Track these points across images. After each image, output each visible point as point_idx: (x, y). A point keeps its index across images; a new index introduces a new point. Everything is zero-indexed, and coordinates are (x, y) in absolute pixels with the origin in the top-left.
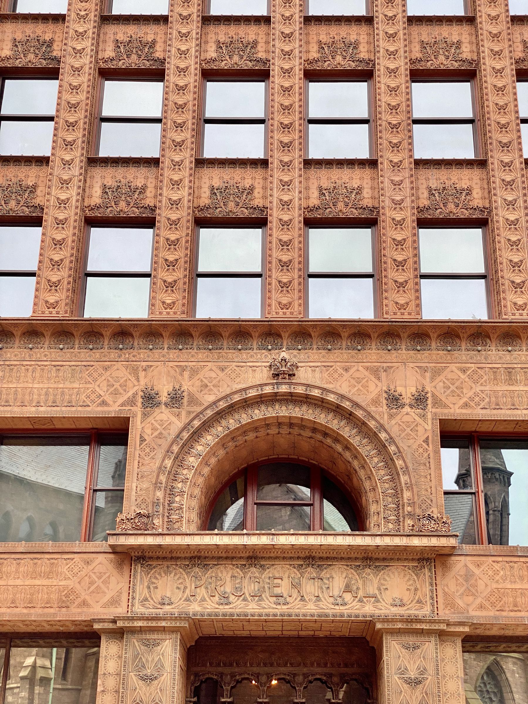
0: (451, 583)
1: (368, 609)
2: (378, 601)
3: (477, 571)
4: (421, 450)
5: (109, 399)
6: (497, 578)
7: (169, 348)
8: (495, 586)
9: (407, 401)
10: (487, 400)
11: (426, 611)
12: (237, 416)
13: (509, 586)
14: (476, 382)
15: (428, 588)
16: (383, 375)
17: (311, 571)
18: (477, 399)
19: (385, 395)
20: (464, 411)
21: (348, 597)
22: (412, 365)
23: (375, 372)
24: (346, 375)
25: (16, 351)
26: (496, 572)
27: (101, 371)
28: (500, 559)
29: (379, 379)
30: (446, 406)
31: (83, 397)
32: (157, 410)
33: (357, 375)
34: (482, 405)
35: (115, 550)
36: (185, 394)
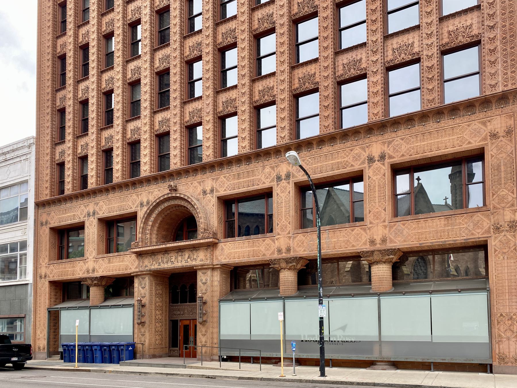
0: (218, 252)
1: (194, 263)
9: (208, 192)
11: (208, 262)
13: (233, 251)
14: (228, 181)
16: (202, 183)
17: (180, 253)
20: (224, 192)
21: (189, 260)
23: (199, 183)
24: (192, 186)
26: (230, 247)
30: (219, 192)
33: (195, 185)
34: (230, 189)
35: (136, 253)
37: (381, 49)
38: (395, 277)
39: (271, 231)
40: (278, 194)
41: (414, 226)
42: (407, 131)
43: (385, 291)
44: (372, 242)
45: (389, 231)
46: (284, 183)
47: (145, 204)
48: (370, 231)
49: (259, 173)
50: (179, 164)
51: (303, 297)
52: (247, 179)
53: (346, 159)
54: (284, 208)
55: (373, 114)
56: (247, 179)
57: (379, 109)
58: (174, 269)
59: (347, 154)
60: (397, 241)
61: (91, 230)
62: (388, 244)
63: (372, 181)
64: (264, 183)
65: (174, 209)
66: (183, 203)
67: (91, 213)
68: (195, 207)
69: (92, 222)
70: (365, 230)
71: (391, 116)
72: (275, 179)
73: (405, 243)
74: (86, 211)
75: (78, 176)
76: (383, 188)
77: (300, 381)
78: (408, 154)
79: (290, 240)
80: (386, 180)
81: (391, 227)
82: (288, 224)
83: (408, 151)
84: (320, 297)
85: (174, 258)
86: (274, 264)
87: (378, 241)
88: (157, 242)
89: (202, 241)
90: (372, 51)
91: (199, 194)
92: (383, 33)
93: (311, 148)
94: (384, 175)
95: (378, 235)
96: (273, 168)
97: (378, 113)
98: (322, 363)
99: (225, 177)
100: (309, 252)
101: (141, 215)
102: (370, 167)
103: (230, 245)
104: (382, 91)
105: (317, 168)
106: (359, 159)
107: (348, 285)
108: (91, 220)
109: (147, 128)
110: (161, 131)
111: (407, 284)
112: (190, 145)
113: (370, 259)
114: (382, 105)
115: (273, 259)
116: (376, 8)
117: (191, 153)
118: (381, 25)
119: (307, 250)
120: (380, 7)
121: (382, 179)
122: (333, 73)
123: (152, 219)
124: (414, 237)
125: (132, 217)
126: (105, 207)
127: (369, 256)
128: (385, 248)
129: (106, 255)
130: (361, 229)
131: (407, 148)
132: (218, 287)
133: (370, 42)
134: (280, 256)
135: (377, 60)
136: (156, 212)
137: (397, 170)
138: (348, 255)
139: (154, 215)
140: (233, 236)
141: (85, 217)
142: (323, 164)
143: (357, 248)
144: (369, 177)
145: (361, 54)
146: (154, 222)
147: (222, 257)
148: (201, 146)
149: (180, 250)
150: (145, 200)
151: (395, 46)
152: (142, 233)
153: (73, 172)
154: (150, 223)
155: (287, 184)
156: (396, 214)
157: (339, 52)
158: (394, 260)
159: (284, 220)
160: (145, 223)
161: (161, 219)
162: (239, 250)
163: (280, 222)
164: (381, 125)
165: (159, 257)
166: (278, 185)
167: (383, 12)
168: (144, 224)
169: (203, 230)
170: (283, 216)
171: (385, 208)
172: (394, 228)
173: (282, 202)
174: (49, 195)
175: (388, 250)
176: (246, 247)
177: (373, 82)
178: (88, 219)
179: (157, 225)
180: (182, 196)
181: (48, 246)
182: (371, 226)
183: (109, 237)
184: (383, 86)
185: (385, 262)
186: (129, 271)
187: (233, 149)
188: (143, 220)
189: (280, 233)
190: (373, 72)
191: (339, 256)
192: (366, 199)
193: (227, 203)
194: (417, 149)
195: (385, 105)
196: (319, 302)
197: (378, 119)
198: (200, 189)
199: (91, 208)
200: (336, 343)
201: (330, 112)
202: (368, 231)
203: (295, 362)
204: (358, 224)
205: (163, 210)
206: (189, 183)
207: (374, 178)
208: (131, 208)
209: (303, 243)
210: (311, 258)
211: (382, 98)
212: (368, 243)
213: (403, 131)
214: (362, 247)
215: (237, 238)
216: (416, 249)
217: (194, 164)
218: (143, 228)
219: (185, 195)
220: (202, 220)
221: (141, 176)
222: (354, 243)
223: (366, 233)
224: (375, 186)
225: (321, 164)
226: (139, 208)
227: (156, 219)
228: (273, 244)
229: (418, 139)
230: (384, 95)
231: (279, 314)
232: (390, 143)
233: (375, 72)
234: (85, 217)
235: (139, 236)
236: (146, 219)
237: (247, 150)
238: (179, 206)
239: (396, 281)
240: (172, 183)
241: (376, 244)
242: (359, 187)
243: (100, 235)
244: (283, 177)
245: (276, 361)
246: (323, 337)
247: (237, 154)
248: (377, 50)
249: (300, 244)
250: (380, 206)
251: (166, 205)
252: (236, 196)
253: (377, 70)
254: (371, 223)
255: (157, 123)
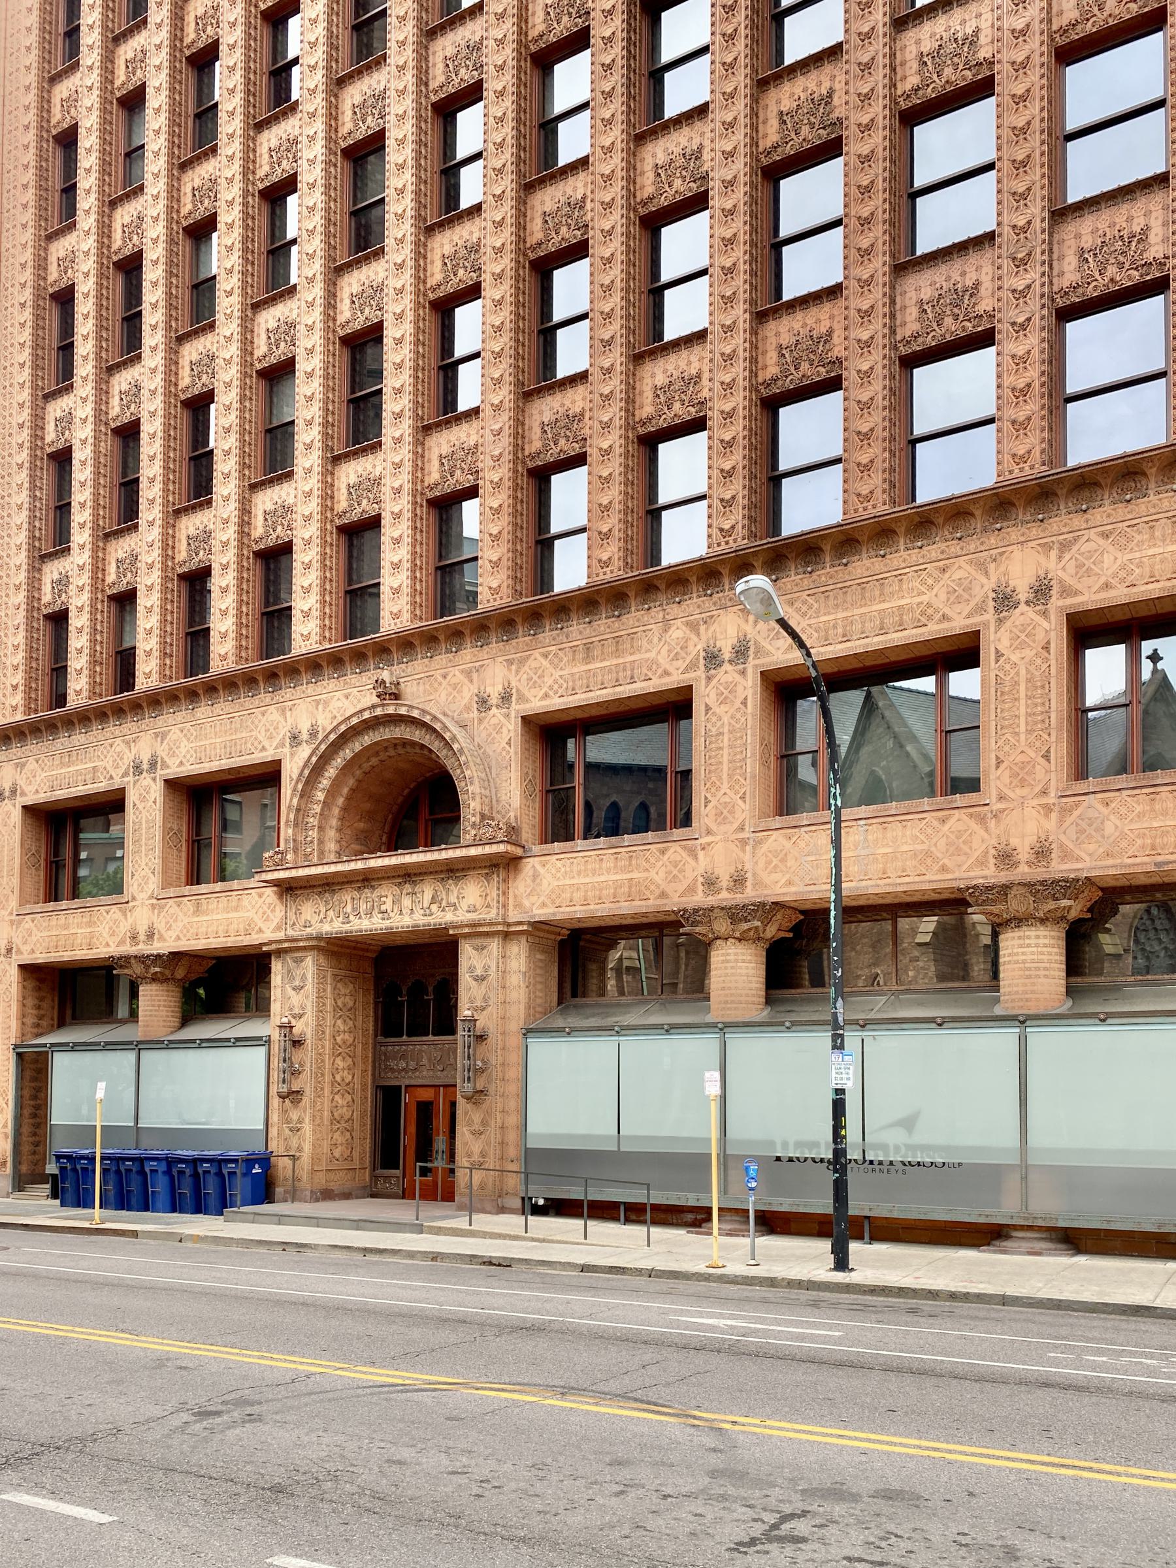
0: (521, 885)
2: (456, 909)
3: (541, 870)
4: (504, 753)
5: (266, 744)
6: (559, 875)
7: (307, 683)
8: (556, 883)
10: (565, 685)
11: (492, 915)
12: (350, 745)
15: (494, 893)
16: (475, 675)
17: (408, 888)
18: (556, 687)
19: (476, 699)
20: (544, 703)
21: (434, 907)
22: (500, 659)
23: (468, 674)
24: (444, 682)
25: (202, 709)
27: (260, 716)
28: (562, 856)
29: (471, 681)
31: (249, 745)
32: (300, 748)
33: (454, 680)
34: (560, 692)
35: (276, 883)
36: (320, 729)
37: (1043, 253)
38: (1074, 965)
39: (686, 820)
40: (708, 709)
41: (1138, 809)
42: (1122, 511)
43: (1042, 1011)
44: (1006, 857)
45: (1061, 822)
46: (727, 673)
47: (305, 736)
48: (998, 822)
49: (650, 641)
50: (406, 616)
51: (782, 1024)
52: (615, 662)
53: (925, 598)
54: (726, 751)
55: (1014, 455)
56: (615, 662)
57: (1033, 442)
58: (390, 934)
59: (930, 581)
60: (1083, 855)
61: (144, 813)
62: (1053, 863)
63: (1008, 667)
64: (666, 673)
65: (392, 752)
66: (417, 735)
67: (145, 762)
68: (455, 746)
69: (147, 790)
70: (981, 820)
71: (1071, 463)
72: (702, 661)
73: (1110, 862)
74: (129, 757)
75: (105, 652)
76: (1043, 687)
77: (772, 1282)
78: (1123, 580)
79: (744, 851)
80: (1053, 662)
81: (1065, 811)
82: (740, 802)
83: (1122, 574)
84: (836, 1026)
85: (389, 901)
86: (694, 924)
87: (1024, 854)
88: (339, 854)
89: (473, 852)
90: (1014, 259)
91: (468, 708)
92: (1050, 200)
93: (817, 563)
94: (1046, 648)
95: (1023, 836)
96: (694, 627)
97: (1029, 452)
98: (840, 1229)
99: (545, 656)
100: (802, 889)
101: (291, 771)
102: (1000, 621)
103: (559, 864)
104: (1043, 385)
105: (835, 627)
106: (966, 596)
107: (927, 991)
108: (145, 783)
109: (313, 506)
110: (355, 516)
111: (1113, 990)
112: (441, 557)
113: (995, 909)
114: (1043, 430)
115: (689, 906)
116: (1029, 123)
117: (443, 583)
118: (1043, 176)
119: (796, 879)
120: (1042, 120)
121: (1039, 661)
122: (886, 331)
123: (325, 783)
124: (1139, 842)
125: (266, 777)
126: (185, 746)
127: (994, 902)
128: (1047, 876)
129: (187, 890)
130: (971, 815)
131: (1119, 562)
132: (523, 990)
133: (1007, 230)
134: (711, 900)
135: (1029, 287)
136: (338, 762)
137: (1087, 631)
138: (926, 898)
139: (331, 772)
140: (569, 837)
141: (126, 774)
142: (849, 617)
143: (957, 875)
144: (999, 655)
145: (977, 270)
146: (331, 793)
147: (534, 899)
148: (476, 559)
149: (408, 876)
150: (304, 728)
151: (1087, 242)
152: (296, 825)
153: (93, 641)
154: (320, 796)
155: (738, 678)
156: (1081, 769)
157: (907, 263)
158: (1073, 915)
159: (725, 788)
160: (306, 794)
161: (351, 782)
162: (587, 880)
163: (714, 795)
164: (1038, 490)
165: (346, 896)
166: (709, 679)
167: (1050, 135)
168: (301, 796)
169: (477, 819)
170: (725, 776)
171: (1048, 751)
172: (1076, 813)
173: (722, 734)
174: (21, 709)
175: (1055, 882)
176: (608, 871)
177: (1013, 356)
178: (135, 783)
179: (340, 801)
180: (415, 714)
181: (17, 861)
182: (1000, 806)
183: (198, 834)
184: (1045, 367)
185: (1043, 921)
186: (254, 939)
187: (571, 570)
188: (300, 786)
189: (714, 827)
190: (1014, 324)
191: (897, 901)
192: (989, 720)
193: (551, 734)
194: (1152, 566)
195: (1051, 429)
196: (835, 1037)
197: (1027, 471)
198: (468, 693)
199: (144, 749)
200: (885, 1167)
201: (875, 451)
202: (992, 824)
203: (756, 1224)
204: (959, 799)
205: (357, 756)
206: (438, 674)
207: (1014, 658)
208: (264, 749)
209: (784, 860)
210: (808, 906)
211: (1043, 407)
212: (992, 861)
213: (1107, 512)
214: (972, 874)
215: (580, 844)
216: (1144, 880)
217: (453, 616)
218: (298, 810)
219: (424, 711)
220: (474, 788)
221: (294, 652)
222: (946, 861)
223: (986, 830)
224: (1017, 683)
225: (845, 614)
226: (287, 750)
227: (336, 783)
228: (693, 863)
229: (1158, 534)
230: (1050, 396)
231: (707, 1075)
232: (1065, 547)
233: (1022, 325)
234: (126, 774)
235: (287, 832)
236: (307, 783)
237: (614, 573)
238: (406, 743)
239: (1079, 979)
240: (385, 675)
241: (1015, 865)
242: (964, 683)
243: (171, 829)
244: (727, 655)
245: (695, 1218)
246: (844, 1151)
247: (583, 583)
248: (1029, 254)
249: (775, 861)
250: (1030, 745)
251: (367, 739)
252: (580, 715)
253: (1029, 319)
254: (1001, 798)
255: (344, 491)
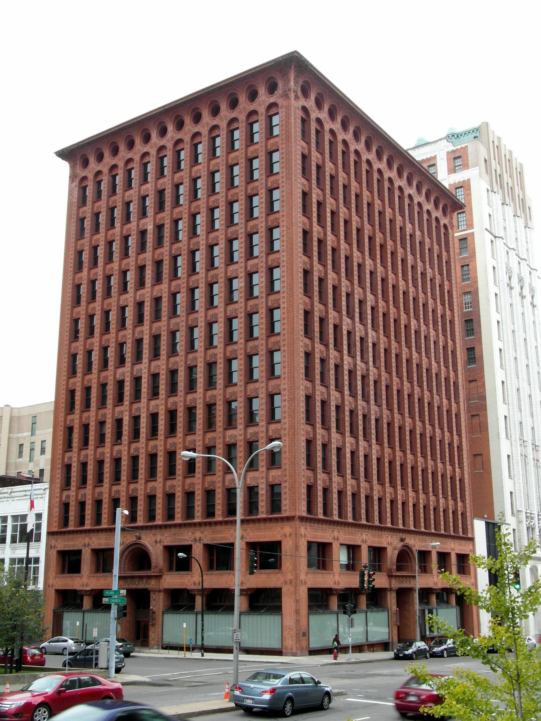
0: (162, 580)
139: (126, 553)
146: (126, 557)
149: (141, 577)
165: (129, 580)
198: (154, 539)
